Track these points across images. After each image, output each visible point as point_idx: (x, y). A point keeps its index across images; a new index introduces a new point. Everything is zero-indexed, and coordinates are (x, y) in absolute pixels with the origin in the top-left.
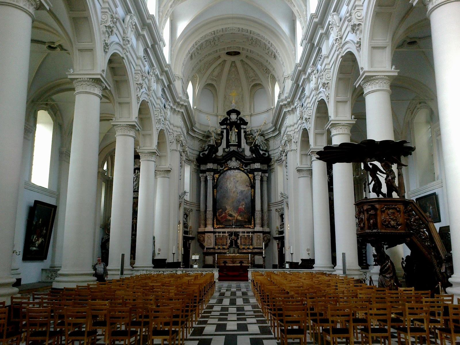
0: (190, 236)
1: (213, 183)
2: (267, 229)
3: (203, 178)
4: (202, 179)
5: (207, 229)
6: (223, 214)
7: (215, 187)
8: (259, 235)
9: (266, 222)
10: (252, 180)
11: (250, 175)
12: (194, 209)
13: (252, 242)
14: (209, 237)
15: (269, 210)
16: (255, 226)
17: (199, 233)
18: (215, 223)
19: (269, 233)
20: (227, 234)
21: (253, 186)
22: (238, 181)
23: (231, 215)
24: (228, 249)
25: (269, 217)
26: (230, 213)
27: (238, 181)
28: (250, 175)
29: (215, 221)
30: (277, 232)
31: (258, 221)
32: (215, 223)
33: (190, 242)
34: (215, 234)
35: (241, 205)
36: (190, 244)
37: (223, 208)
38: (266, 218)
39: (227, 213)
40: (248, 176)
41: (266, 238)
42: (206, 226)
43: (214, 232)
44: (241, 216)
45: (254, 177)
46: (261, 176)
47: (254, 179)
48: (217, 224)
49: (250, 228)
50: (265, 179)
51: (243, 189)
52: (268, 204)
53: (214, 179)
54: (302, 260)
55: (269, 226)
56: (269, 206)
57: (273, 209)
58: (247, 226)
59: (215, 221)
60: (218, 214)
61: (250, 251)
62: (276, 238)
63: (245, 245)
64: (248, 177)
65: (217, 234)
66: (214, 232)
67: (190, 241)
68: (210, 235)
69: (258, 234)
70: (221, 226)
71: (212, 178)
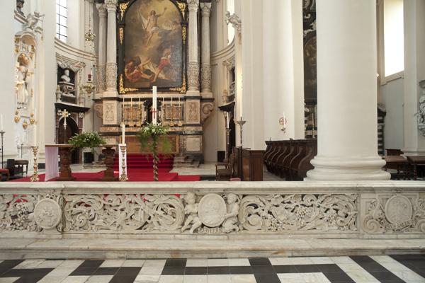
0: (82, 106)
1: (117, 19)
2: (207, 94)
3: (103, 11)
4: (101, 14)
5: (106, 94)
6: (136, 70)
7: (121, 23)
8: (194, 103)
9: (206, 83)
10: (184, 14)
11: (179, 4)
12: (90, 63)
13: (183, 115)
14: (109, 106)
15: (213, 65)
16: (187, 89)
17: (96, 101)
18: (121, 84)
19: (212, 100)
20: (140, 103)
21: (185, 23)
22: (158, 16)
23: (148, 72)
24: (142, 126)
25: (212, 74)
26: (147, 67)
27: (158, 16)
28: (181, 5)
29: (121, 80)
30: (225, 99)
31: (193, 80)
32: (121, 84)
33: (80, 116)
34: (121, 103)
35: (164, 54)
36: (81, 120)
37: (135, 59)
38: (206, 76)
39: (142, 68)
40: (177, 6)
41: (206, 109)
42: (105, 88)
43: (119, 100)
44: (165, 72)
45: (187, 6)
46: (199, 7)
47: (187, 11)
48: (124, 87)
49: (179, 92)
50: (206, 12)
51: (169, 29)
52: (211, 55)
53: (118, 11)
54: (267, 142)
55: (211, 89)
56: (212, 57)
57: (219, 62)
58: (174, 89)
59: (121, 80)
60: (126, 70)
61: (178, 129)
62: (223, 109)
63: (170, 120)
64: (176, 9)
65: (124, 103)
66: (119, 100)
67: (81, 115)
68: (110, 104)
69: (193, 101)
70: (131, 90)
71: (115, 10)
